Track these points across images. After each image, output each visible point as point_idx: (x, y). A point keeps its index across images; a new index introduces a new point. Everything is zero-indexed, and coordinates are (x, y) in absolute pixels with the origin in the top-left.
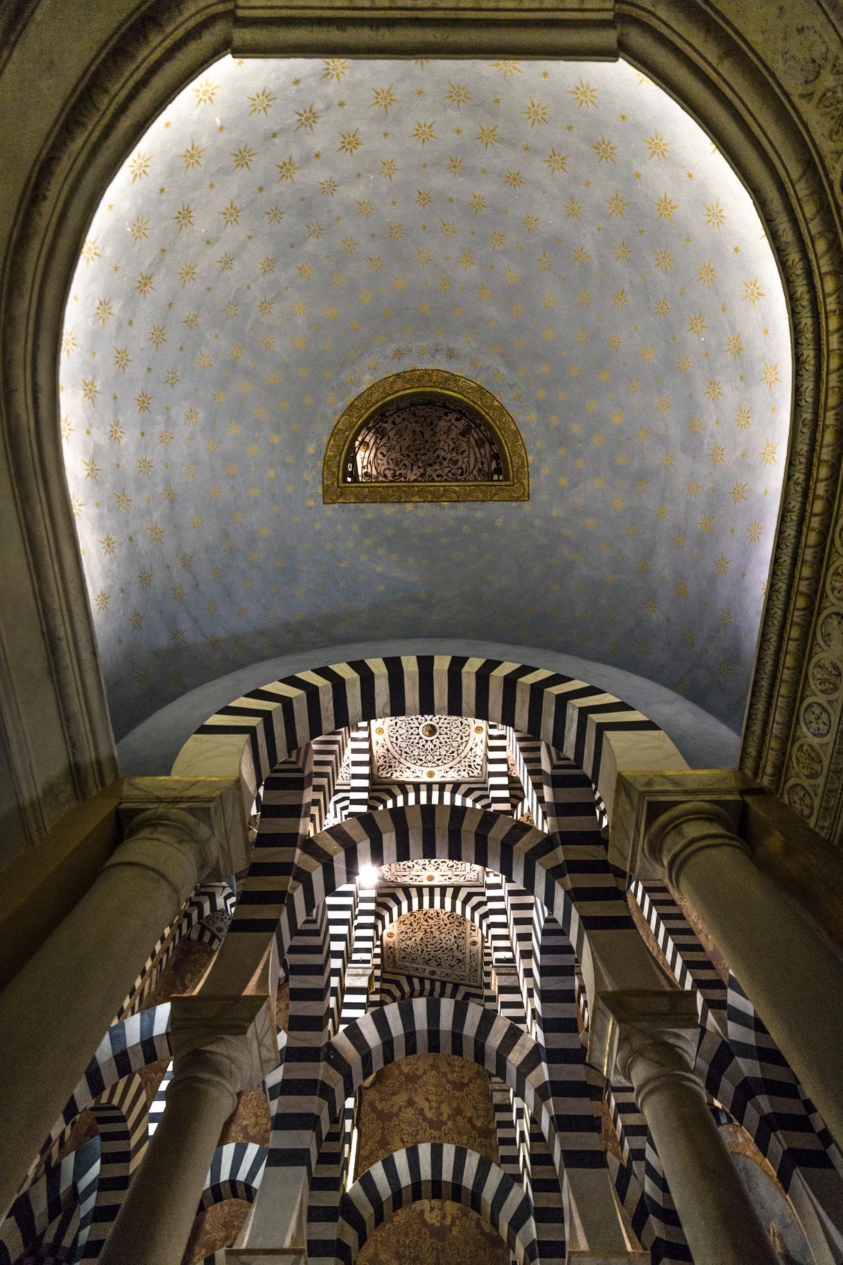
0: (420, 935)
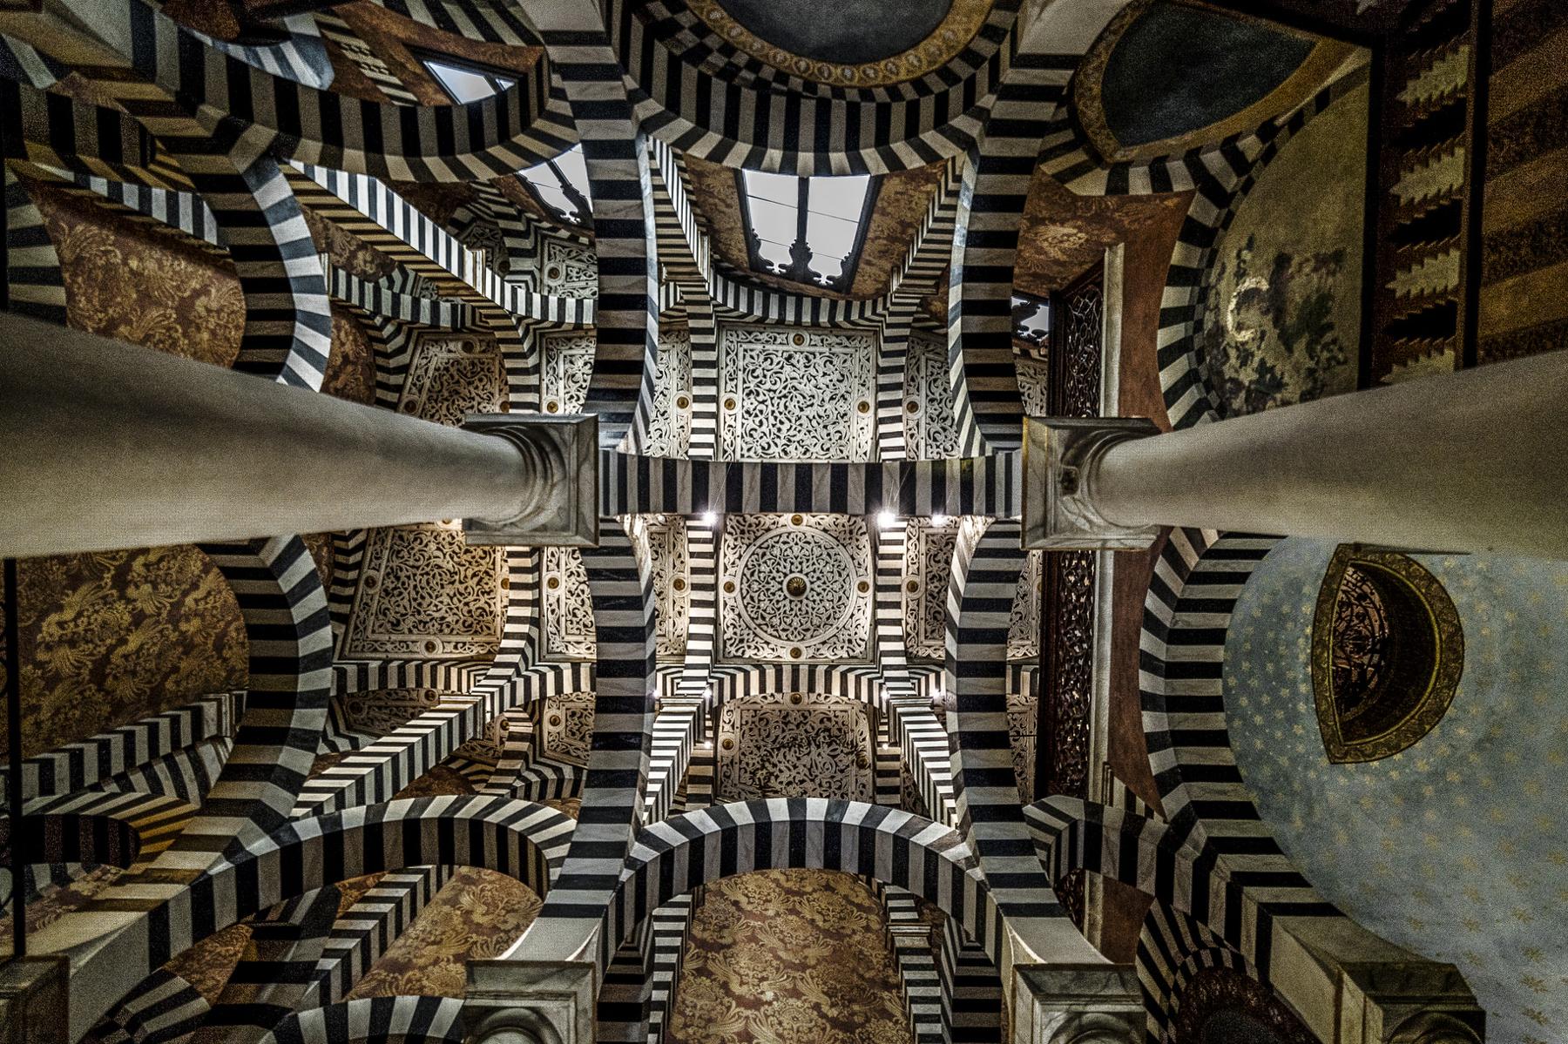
0: (448, 565)
